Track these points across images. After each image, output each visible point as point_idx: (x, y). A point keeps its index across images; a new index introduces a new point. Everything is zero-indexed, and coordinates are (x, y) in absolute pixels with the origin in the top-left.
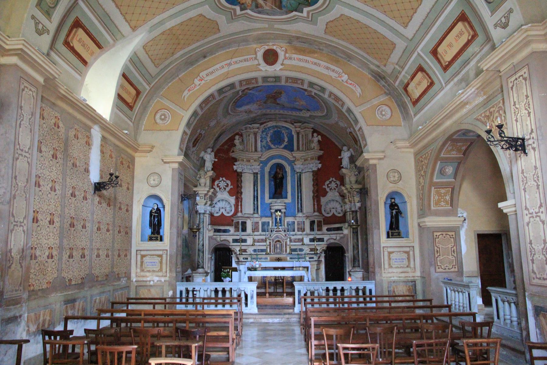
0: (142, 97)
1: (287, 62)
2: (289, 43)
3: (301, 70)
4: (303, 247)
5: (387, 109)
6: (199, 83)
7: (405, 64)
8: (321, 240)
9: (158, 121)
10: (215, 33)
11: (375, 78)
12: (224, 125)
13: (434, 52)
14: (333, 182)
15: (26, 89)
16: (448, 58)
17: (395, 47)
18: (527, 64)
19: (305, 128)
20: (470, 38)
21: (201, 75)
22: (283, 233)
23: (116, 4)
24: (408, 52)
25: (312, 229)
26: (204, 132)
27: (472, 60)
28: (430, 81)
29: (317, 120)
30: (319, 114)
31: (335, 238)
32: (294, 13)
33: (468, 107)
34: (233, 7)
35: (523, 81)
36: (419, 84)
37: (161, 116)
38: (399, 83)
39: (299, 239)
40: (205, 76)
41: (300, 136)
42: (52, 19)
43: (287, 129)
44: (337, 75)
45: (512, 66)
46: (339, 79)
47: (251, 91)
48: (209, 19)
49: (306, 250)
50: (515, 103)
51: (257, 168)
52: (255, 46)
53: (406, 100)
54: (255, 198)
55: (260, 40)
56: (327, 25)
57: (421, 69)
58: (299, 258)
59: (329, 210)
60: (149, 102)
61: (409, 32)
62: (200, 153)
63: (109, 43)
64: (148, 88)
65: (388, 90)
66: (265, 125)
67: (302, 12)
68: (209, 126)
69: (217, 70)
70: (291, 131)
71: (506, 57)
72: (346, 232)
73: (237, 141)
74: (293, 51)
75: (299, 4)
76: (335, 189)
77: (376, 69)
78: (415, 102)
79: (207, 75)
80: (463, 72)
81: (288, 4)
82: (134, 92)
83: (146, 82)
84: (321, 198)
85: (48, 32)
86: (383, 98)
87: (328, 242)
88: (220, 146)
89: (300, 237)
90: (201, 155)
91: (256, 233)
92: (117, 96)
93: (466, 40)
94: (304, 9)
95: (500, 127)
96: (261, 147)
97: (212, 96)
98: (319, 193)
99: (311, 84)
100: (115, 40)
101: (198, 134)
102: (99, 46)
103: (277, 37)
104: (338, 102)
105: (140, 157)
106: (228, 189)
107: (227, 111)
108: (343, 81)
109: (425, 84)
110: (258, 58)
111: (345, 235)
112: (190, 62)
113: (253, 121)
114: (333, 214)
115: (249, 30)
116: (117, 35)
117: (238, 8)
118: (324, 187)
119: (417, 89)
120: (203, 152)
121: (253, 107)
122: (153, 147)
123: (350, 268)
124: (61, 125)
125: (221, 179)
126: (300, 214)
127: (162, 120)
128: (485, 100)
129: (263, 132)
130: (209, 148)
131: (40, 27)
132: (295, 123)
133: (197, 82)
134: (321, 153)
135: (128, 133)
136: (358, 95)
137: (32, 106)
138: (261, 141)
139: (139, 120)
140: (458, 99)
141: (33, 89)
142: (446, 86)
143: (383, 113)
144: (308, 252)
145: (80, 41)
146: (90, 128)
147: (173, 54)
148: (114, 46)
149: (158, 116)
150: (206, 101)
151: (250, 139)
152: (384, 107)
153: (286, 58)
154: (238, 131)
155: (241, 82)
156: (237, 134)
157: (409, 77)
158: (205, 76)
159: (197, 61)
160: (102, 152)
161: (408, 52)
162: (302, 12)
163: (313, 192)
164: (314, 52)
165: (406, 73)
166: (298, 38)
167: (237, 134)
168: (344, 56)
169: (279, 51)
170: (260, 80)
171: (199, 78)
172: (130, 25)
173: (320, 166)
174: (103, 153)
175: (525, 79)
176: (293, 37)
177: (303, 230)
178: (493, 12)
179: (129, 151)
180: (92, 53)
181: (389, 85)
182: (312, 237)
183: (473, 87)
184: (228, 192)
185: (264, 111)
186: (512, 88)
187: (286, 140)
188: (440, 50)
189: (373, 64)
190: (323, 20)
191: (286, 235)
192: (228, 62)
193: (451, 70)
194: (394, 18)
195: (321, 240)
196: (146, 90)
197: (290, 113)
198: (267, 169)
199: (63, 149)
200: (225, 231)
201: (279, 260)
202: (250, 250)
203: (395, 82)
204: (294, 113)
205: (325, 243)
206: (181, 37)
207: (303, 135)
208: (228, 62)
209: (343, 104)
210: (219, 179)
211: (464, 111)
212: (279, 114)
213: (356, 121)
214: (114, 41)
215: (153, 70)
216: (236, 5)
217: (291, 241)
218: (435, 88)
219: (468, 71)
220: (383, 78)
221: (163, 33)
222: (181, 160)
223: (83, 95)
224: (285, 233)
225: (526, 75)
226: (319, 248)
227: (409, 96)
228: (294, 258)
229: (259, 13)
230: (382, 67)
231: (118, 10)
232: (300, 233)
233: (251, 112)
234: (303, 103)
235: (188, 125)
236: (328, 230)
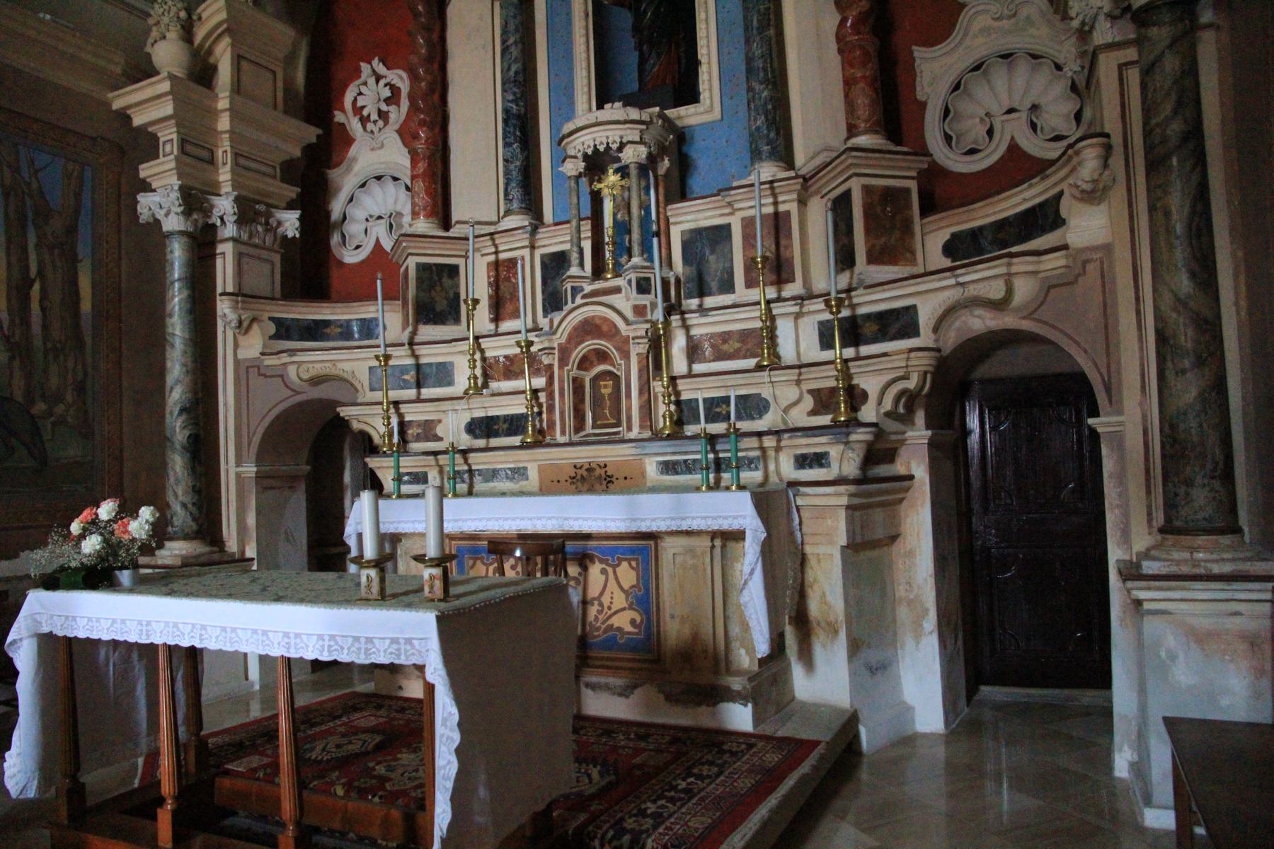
4: (762, 386)
8: (898, 323)
22: (626, 301)
31: (996, 291)
39: (745, 335)
49: (788, 401)
54: (520, 127)
58: (719, 465)
72: (1087, 226)
84: (918, 52)
87: (951, 340)
89: (750, 320)
106: (398, 114)
111: (1081, 260)
114: (1014, 148)
123: (1142, 540)
125: (365, 67)
144: (800, 417)
177: (779, 270)
191: (639, 310)
195: (898, 323)
201: (592, 480)
202: (453, 428)
205: (925, 338)
210: (357, 73)
217: (693, 352)
226: (870, 383)
228: (688, 467)
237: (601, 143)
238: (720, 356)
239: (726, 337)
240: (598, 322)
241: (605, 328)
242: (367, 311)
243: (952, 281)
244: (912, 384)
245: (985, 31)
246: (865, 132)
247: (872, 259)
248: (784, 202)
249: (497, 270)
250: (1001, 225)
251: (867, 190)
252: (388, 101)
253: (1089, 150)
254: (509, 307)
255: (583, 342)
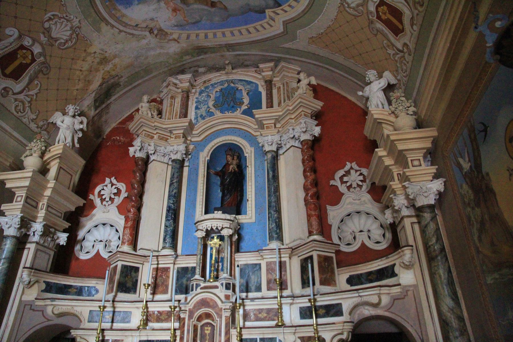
8: (334, 310)
14: (352, 172)
22: (221, 292)
25: (305, 283)
31: (375, 300)
39: (269, 311)
41: (275, 91)
43: (249, 83)
51: (176, 148)
54: (173, 213)
59: (351, 237)
70: (257, 85)
72: (407, 277)
76: (358, 185)
84: (328, 207)
87: (356, 318)
88: (120, 123)
89: (273, 304)
91: (158, 297)
98: (320, 197)
106: (118, 200)
111: (406, 290)
114: (363, 245)
118: (332, 182)
125: (108, 180)
126: (275, 245)
134: (318, 105)
138: (197, 108)
163: (306, 189)
173: (317, 131)
177: (282, 285)
182: (305, 303)
184: (118, 207)
191: (227, 297)
195: (334, 310)
198: (204, 156)
200: (79, 291)
205: (345, 317)
210: (104, 181)
217: (246, 317)
224: (230, 292)
232: (276, 293)
236: (351, 281)
237: (214, 226)
238: (258, 319)
239: (260, 311)
240: (208, 300)
241: (211, 304)
242: (91, 283)
243: (357, 295)
244: (344, 337)
245: (350, 203)
246: (317, 234)
247: (322, 283)
248: (284, 257)
249: (157, 271)
250: (370, 273)
251: (319, 256)
252: (115, 194)
253: (407, 251)
254: (160, 289)
255: (201, 309)
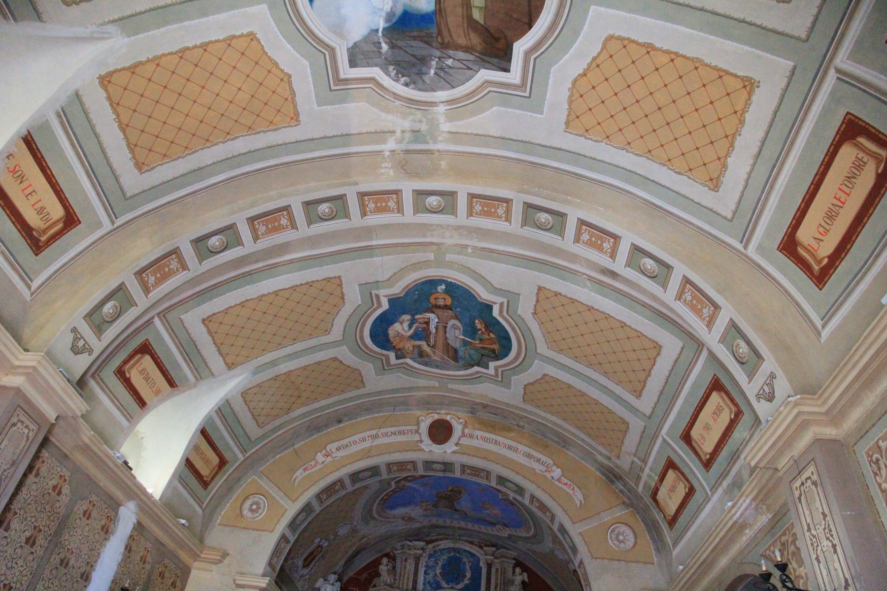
0: (229, 470)
1: (465, 441)
2: (472, 413)
3: (486, 455)
5: (629, 532)
6: (323, 459)
7: (648, 454)
9: (246, 512)
10: (357, 388)
11: (608, 477)
12: (363, 538)
13: (687, 438)
15: (19, 425)
16: (708, 447)
17: (628, 428)
18: (813, 459)
19: (502, 557)
20: (732, 417)
21: (328, 448)
23: (208, 329)
24: (649, 437)
26: (326, 544)
27: (741, 452)
28: (687, 485)
29: (521, 545)
30: (523, 534)
32: (476, 369)
33: (749, 533)
34: (385, 352)
35: (813, 487)
36: (672, 489)
37: (251, 505)
38: (644, 488)
40: (334, 450)
41: (493, 570)
42: (103, 337)
43: (473, 555)
44: (544, 469)
45: (792, 462)
46: (547, 474)
47: (408, 484)
48: (349, 367)
50: (808, 525)
52: (419, 413)
53: (659, 517)
55: (427, 404)
56: (525, 389)
57: (671, 465)
60: (239, 480)
61: (646, 404)
62: (316, 581)
63: (187, 380)
64: (241, 457)
65: (629, 498)
66: (434, 544)
67: (487, 368)
68: (336, 535)
69: (355, 442)
71: (780, 444)
73: (383, 568)
74: (477, 426)
75: (483, 355)
77: (606, 462)
78: (672, 522)
79: (338, 449)
80: (733, 472)
81: (467, 355)
82: (215, 460)
83: (238, 447)
85: (91, 351)
86: (620, 512)
88: (357, 573)
90: (317, 585)
92: (184, 462)
93: (727, 421)
94: (490, 363)
95: (782, 567)
96: (424, 584)
97: (340, 481)
99: (501, 480)
100: (199, 377)
101: (315, 545)
102: (172, 383)
103: (452, 403)
104: (545, 513)
105: (199, 569)
107: (371, 510)
108: (553, 477)
109: (681, 490)
110: (420, 431)
112: (315, 427)
113: (416, 535)
115: (410, 389)
116: (202, 371)
117: (392, 355)
119: (671, 498)
120: (321, 580)
121: (415, 511)
122: (225, 555)
124: (66, 489)
127: (251, 510)
128: (771, 520)
129: (430, 556)
130: (335, 573)
131: (81, 343)
132: (486, 546)
133: (320, 457)
135: (187, 524)
136: (578, 503)
137: (18, 451)
138: (426, 573)
139: (216, 508)
140: (728, 517)
141: (32, 426)
142: (712, 495)
143: (621, 538)
145: (142, 372)
146: (119, 505)
147: (289, 410)
148: (195, 386)
149: (247, 505)
150: (330, 489)
151: (408, 565)
152: (623, 528)
153: (463, 435)
154: (388, 550)
155: (389, 465)
156: (387, 555)
157: (657, 478)
158: (334, 450)
159: (327, 426)
160: (128, 549)
161: (649, 437)
162: (487, 368)
164: (510, 430)
165: (651, 470)
166: (485, 406)
167: (387, 555)
168: (556, 439)
169: (454, 423)
170: (420, 466)
171: (324, 451)
172: (224, 360)
174: (130, 551)
175: (814, 483)
176: (477, 404)
178: (751, 376)
179: (184, 556)
180: (158, 392)
181: (629, 490)
183: (747, 496)
185: (434, 521)
186: (799, 498)
187: (468, 575)
188: (694, 433)
189: (601, 454)
190: (519, 381)
192: (374, 432)
193: (716, 467)
194: (619, 383)
196: (238, 459)
197: (476, 527)
199: (52, 532)
203: (637, 484)
204: (483, 529)
206: (302, 387)
207: (497, 570)
208: (374, 432)
209: (553, 517)
211: (744, 539)
212: (460, 528)
213: (574, 550)
214: (197, 379)
215: (254, 431)
216: (388, 350)
218: (697, 497)
219: (740, 471)
220: (619, 478)
221: (275, 378)
222: (264, 585)
223: (127, 450)
225: (815, 477)
227: (661, 511)
229: (426, 364)
230: (614, 459)
231: (210, 338)
233: (411, 519)
234: (496, 511)
235: (292, 525)
